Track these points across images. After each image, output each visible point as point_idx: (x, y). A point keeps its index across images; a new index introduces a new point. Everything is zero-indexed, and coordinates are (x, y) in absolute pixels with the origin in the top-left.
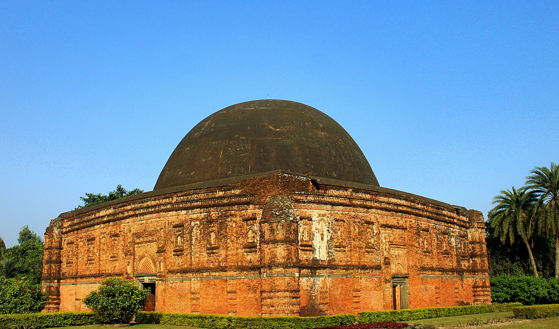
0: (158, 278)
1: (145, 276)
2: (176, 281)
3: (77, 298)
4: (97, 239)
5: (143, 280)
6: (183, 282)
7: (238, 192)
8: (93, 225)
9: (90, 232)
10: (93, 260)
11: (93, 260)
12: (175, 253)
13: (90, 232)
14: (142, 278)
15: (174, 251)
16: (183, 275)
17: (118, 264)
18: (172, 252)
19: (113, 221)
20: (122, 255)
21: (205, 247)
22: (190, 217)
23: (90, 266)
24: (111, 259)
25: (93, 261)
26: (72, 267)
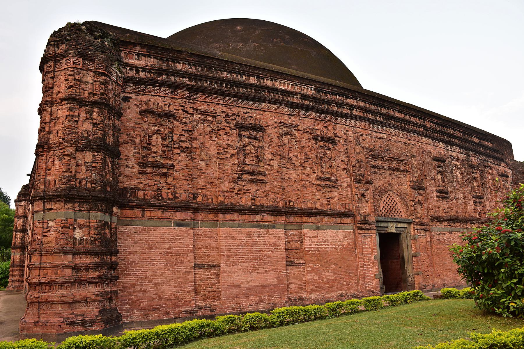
0: (419, 227)
1: (390, 222)
2: (444, 232)
3: (198, 262)
4: (271, 131)
5: (387, 227)
6: (452, 233)
7: (490, 145)
8: (262, 100)
9: (245, 111)
10: (264, 174)
11: (264, 174)
12: (439, 194)
13: (245, 111)
14: (385, 225)
15: (437, 191)
16: (451, 224)
17: (337, 194)
18: (435, 192)
19: (321, 112)
20: (346, 180)
21: (470, 193)
22: (450, 154)
23: (253, 187)
24: (318, 182)
25: (263, 178)
26: (170, 180)
